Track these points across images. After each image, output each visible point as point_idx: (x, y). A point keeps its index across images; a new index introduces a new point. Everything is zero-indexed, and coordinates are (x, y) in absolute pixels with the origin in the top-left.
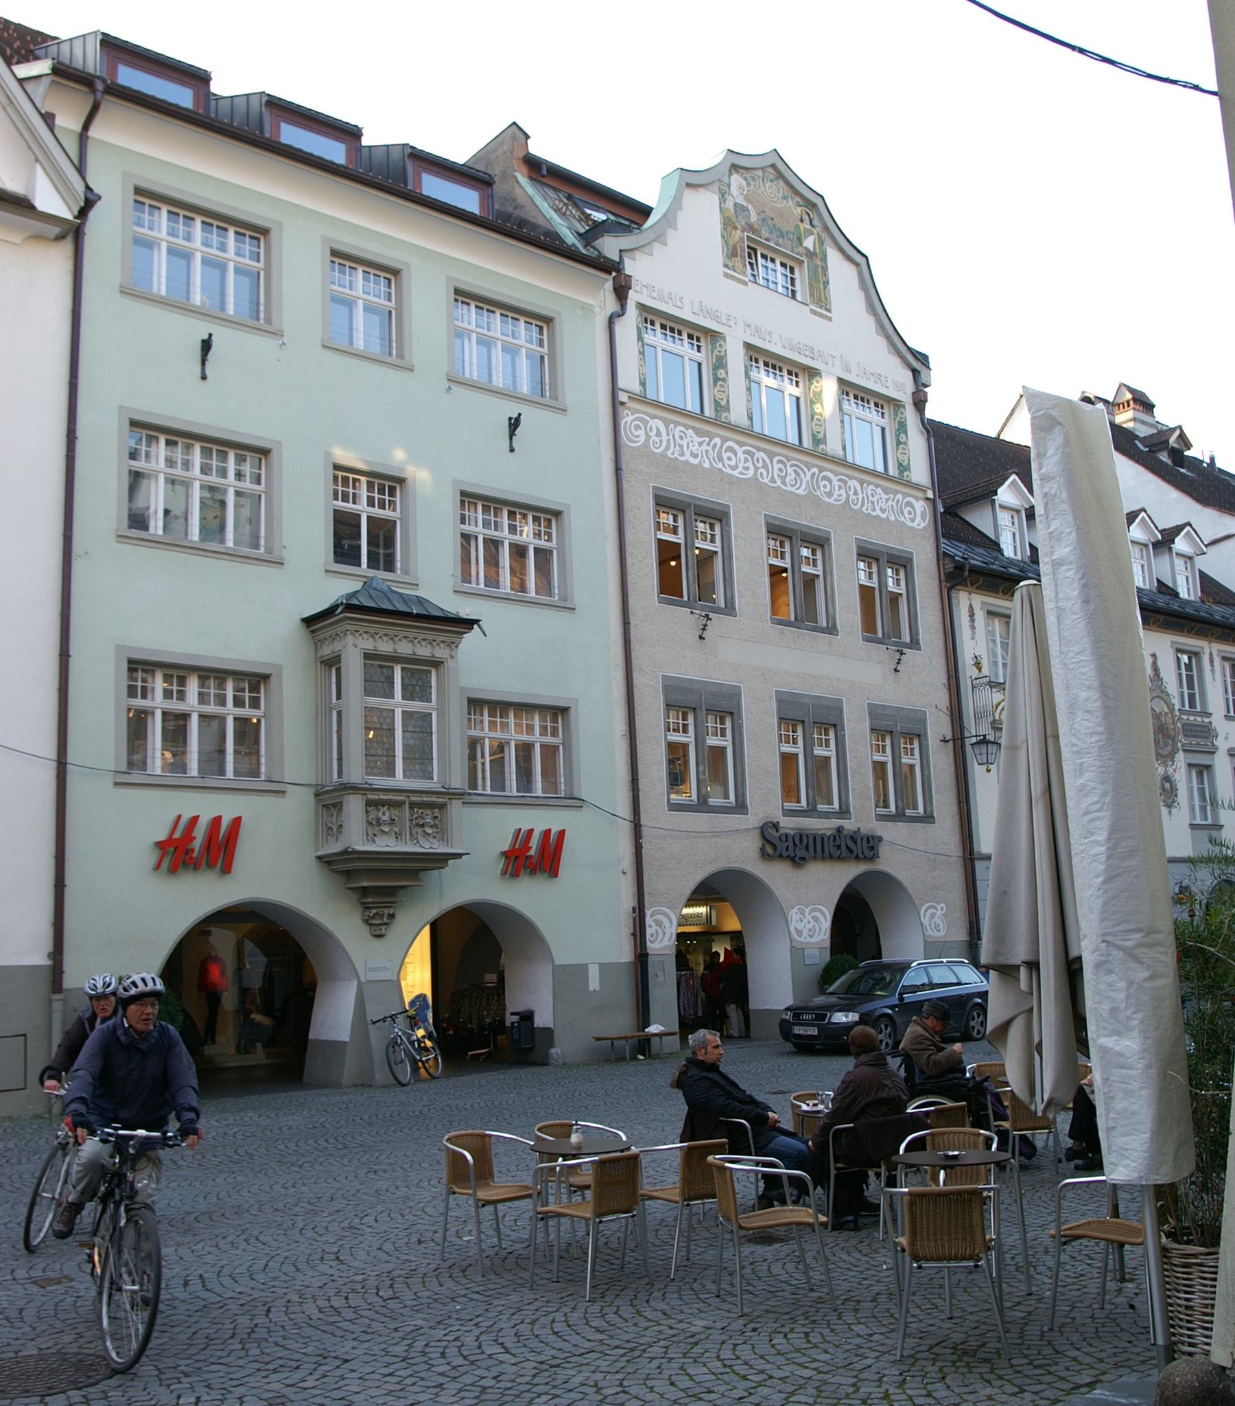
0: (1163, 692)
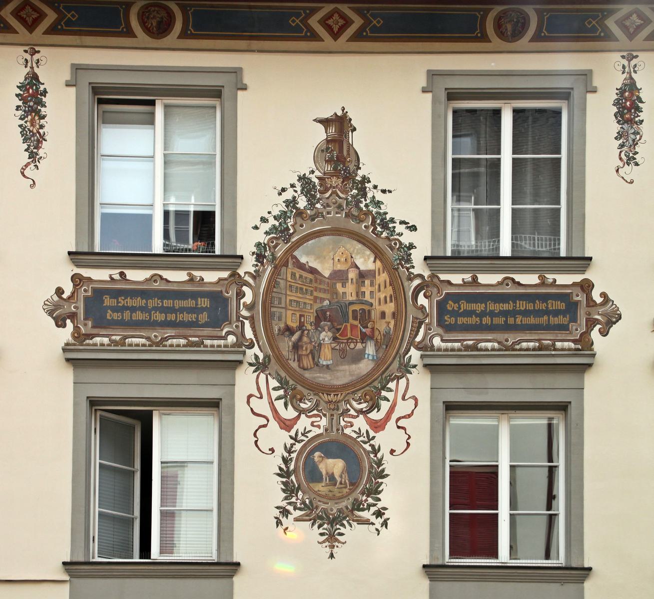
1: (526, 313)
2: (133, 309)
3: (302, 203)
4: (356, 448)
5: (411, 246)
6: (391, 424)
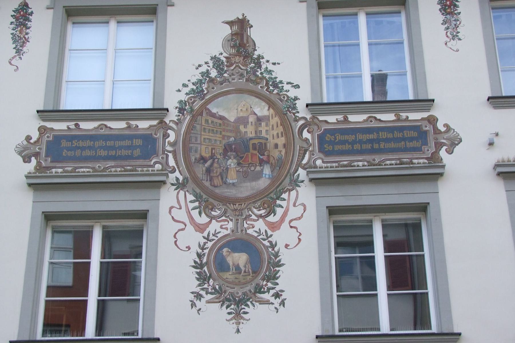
1: (387, 140)
2: (83, 149)
3: (214, 73)
4: (257, 244)
5: (296, 99)
6: (285, 225)
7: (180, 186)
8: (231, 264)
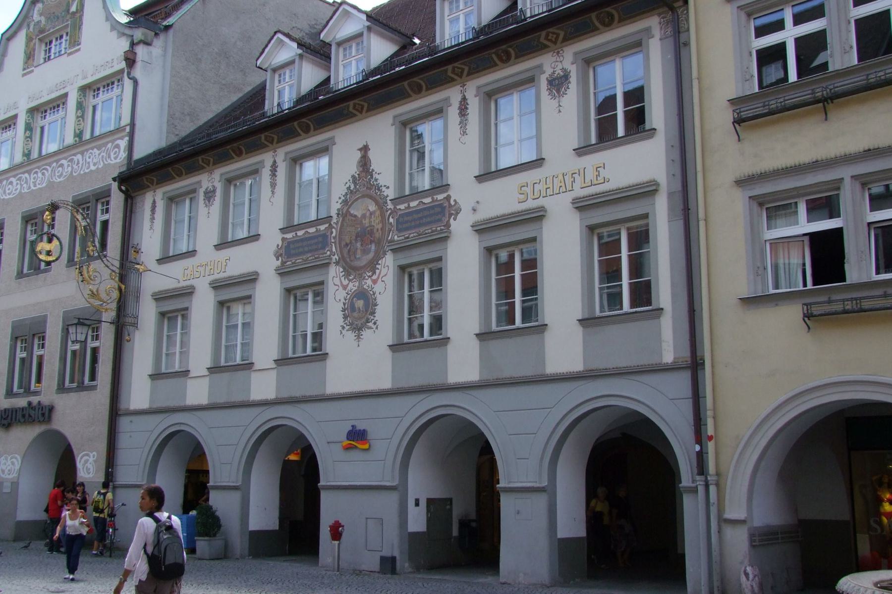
0: (370, 187)
1: (426, 217)
5: (387, 196)
6: (380, 280)
7: (337, 263)
8: (356, 306)
